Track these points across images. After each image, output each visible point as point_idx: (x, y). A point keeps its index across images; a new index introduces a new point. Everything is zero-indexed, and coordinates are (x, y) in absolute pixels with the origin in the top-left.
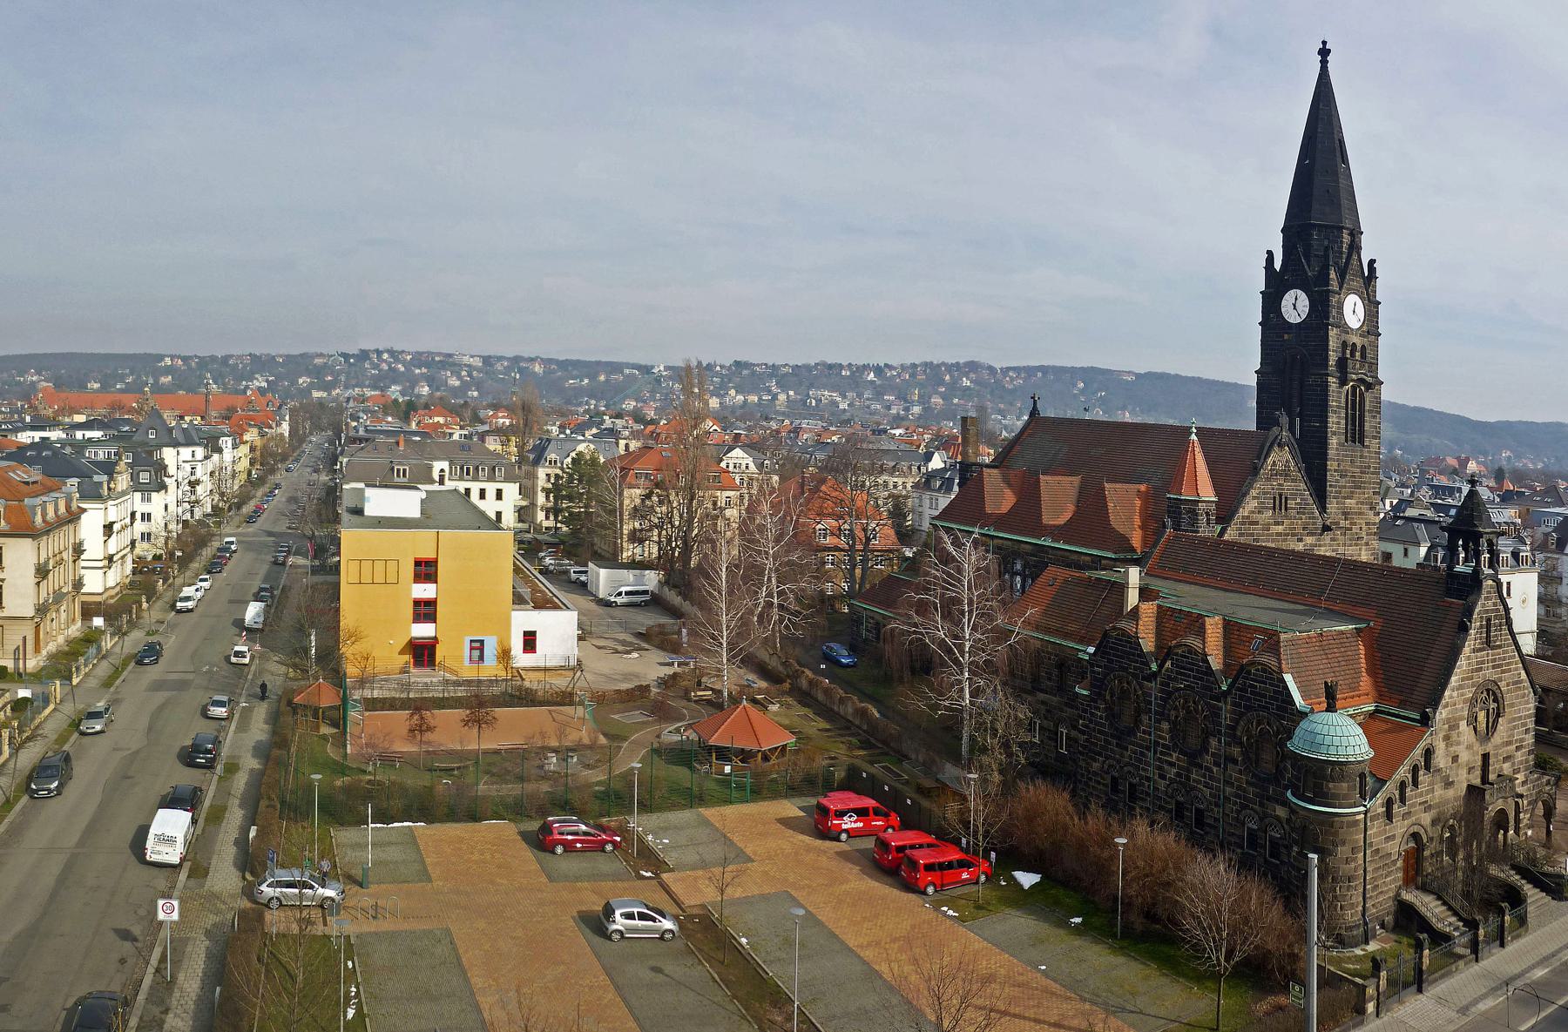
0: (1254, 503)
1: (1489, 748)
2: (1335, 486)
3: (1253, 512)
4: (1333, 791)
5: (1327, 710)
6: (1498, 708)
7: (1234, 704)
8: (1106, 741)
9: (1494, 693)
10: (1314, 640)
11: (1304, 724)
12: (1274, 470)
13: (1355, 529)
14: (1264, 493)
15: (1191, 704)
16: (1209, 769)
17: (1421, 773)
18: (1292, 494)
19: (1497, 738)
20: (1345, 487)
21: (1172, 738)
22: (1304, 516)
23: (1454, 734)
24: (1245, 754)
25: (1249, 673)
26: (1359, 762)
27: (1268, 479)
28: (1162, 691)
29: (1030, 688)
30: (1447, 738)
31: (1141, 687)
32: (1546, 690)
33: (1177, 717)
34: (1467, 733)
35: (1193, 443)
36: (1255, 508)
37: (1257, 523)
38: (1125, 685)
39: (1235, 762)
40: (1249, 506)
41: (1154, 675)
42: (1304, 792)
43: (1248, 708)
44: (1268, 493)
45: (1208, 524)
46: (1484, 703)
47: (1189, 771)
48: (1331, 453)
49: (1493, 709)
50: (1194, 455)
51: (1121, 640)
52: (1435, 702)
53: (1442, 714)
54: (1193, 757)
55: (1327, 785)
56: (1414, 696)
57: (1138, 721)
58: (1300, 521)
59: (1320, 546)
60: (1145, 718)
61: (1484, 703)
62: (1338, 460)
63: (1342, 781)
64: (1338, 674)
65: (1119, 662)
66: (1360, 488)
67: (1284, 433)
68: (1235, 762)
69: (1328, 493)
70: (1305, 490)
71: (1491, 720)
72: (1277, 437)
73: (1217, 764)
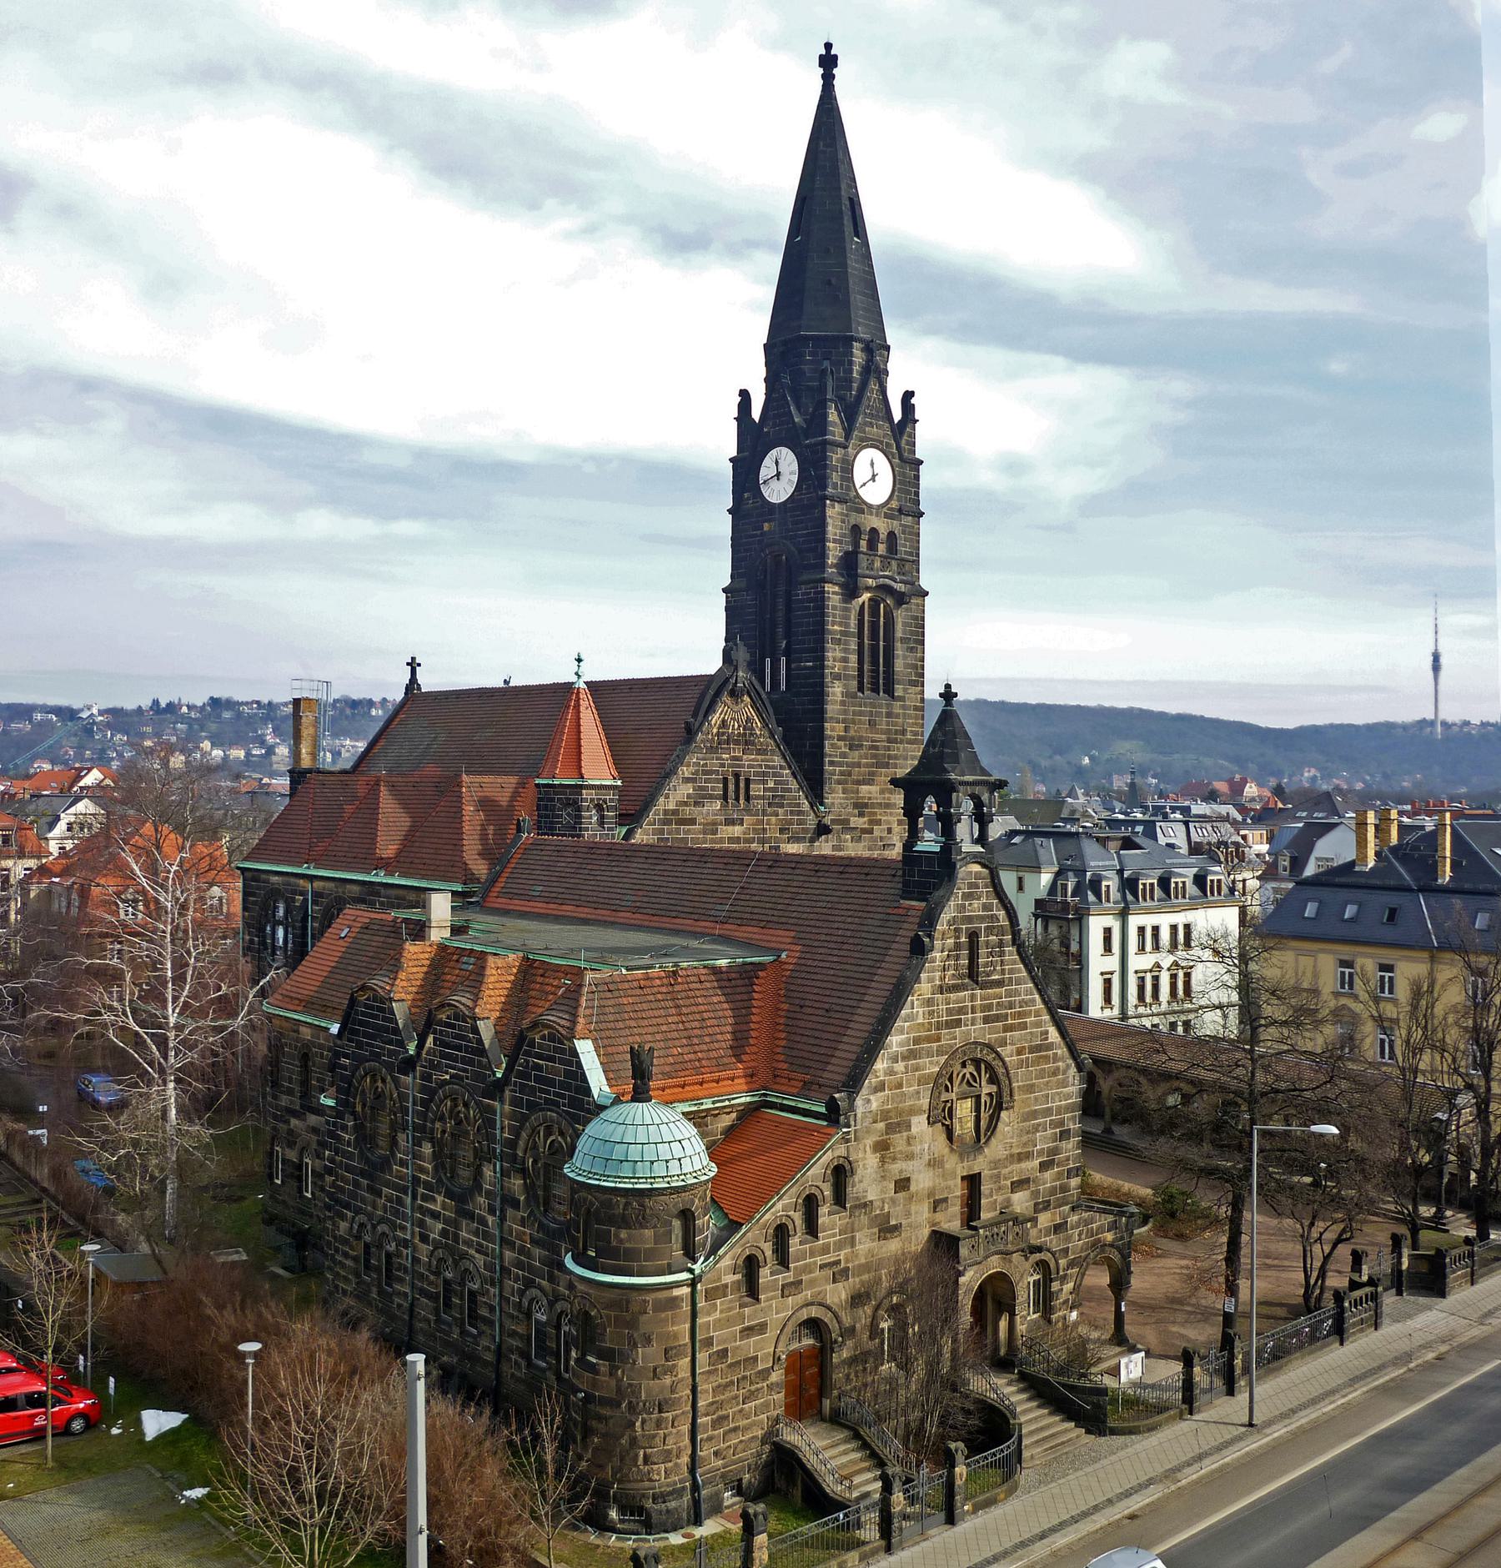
0: (689, 789)
1: (979, 1164)
2: (840, 764)
3: (685, 804)
4: (627, 1245)
5: (634, 1100)
6: (1000, 1094)
7: (515, 1102)
8: (356, 1184)
9: (989, 1067)
10: (658, 982)
11: (594, 1128)
12: (723, 734)
13: (878, 831)
14: (705, 773)
15: (461, 1108)
16: (483, 1221)
17: (823, 1210)
18: (756, 774)
19: (996, 1148)
20: (859, 765)
21: (436, 1168)
23: (898, 1141)
24: (529, 1189)
25: (532, 1044)
26: (684, 1189)
27: (711, 750)
28: (423, 1089)
29: (298, 1108)
30: (882, 1147)
31: (396, 1081)
32: (1104, 1064)
33: (444, 1132)
34: (928, 1138)
35: (578, 693)
36: (689, 796)
37: (692, 822)
38: (380, 1084)
39: (515, 1204)
40: (677, 793)
41: (409, 1065)
42: (585, 1249)
43: (532, 1106)
45: (601, 823)
46: (968, 1083)
47: (457, 1227)
48: (832, 709)
49: (990, 1094)
50: (579, 712)
51: (372, 1007)
52: (853, 1083)
53: (868, 1103)
54: (461, 1198)
55: (617, 1236)
56: (825, 1075)
57: (394, 1143)
58: (773, 819)
60: (401, 1137)
61: (968, 1083)
62: (844, 721)
63: (642, 1227)
64: (696, 1041)
65: (368, 1044)
67: (741, 674)
68: (515, 1204)
69: (826, 776)
70: (782, 767)
71: (984, 1116)
72: (727, 680)
73: (492, 1211)
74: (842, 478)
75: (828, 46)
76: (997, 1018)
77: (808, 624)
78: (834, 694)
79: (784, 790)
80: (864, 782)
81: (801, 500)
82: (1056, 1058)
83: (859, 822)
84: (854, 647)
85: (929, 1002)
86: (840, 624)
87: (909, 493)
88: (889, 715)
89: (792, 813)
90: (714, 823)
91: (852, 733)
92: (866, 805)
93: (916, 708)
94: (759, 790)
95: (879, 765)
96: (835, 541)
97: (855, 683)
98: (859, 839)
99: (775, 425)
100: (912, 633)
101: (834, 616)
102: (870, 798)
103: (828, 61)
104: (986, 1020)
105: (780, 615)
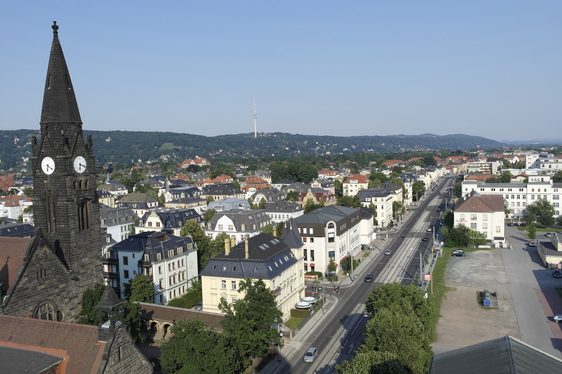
2: (75, 255)
13: (89, 272)
20: (81, 253)
22: (57, 276)
36: (26, 281)
37: (28, 288)
44: (34, 271)
58: (55, 279)
59: (68, 287)
62: (75, 242)
66: (90, 251)
74: (70, 168)
75: (55, 22)
76: (128, 366)
77: (62, 214)
78: (72, 234)
79: (59, 269)
80: (84, 258)
81: (57, 175)
82: (145, 368)
83: (83, 271)
84: (77, 218)
85: (108, 372)
86: (72, 213)
87: (92, 167)
88: (90, 236)
89: (61, 275)
90: (36, 287)
91: (79, 244)
92: (84, 265)
93: (98, 231)
94: (50, 272)
95: (88, 251)
96: (69, 188)
97: (78, 229)
98: (84, 276)
99: (45, 150)
100: (96, 209)
101: (70, 211)
102: (85, 262)
103: (55, 28)
104: (125, 368)
105: (52, 209)
